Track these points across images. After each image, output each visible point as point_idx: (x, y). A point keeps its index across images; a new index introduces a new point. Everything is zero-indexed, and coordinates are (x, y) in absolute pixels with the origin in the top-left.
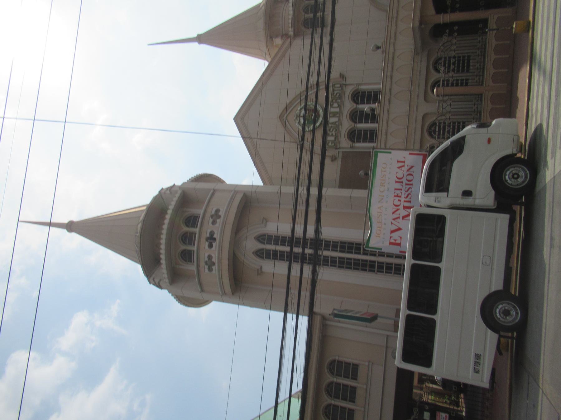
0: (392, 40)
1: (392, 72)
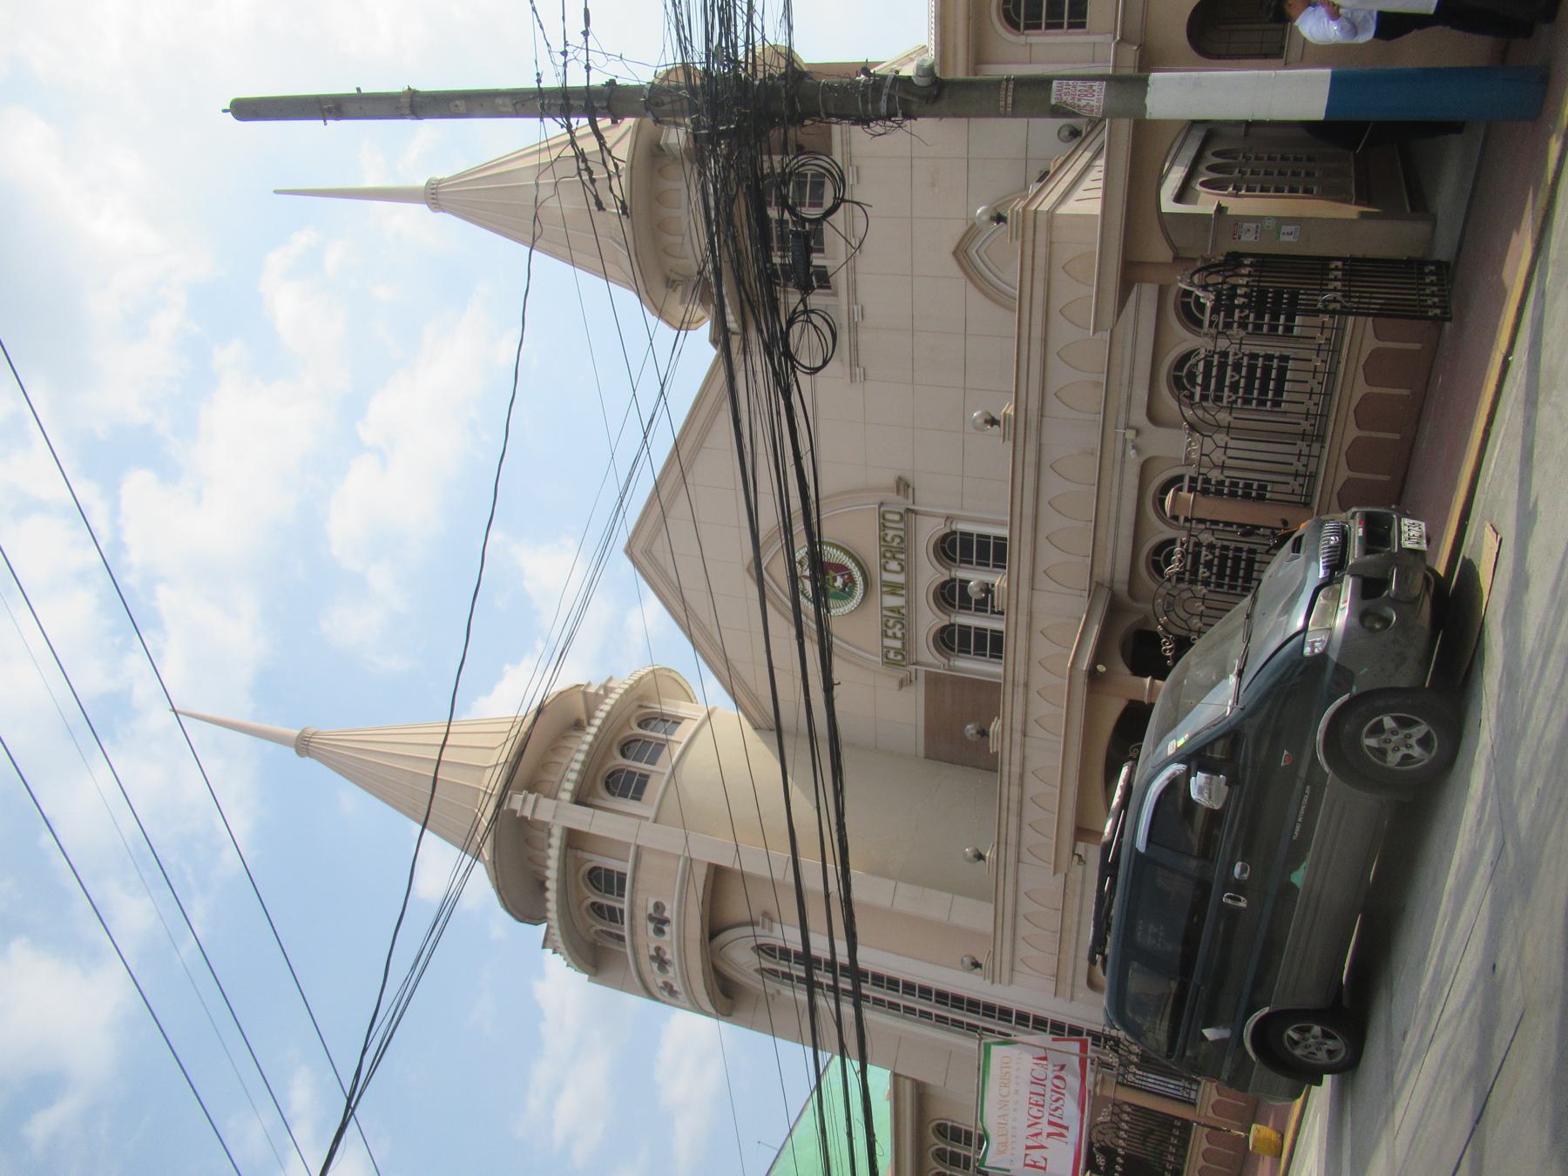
0: (1017, 736)
1: (1021, 802)
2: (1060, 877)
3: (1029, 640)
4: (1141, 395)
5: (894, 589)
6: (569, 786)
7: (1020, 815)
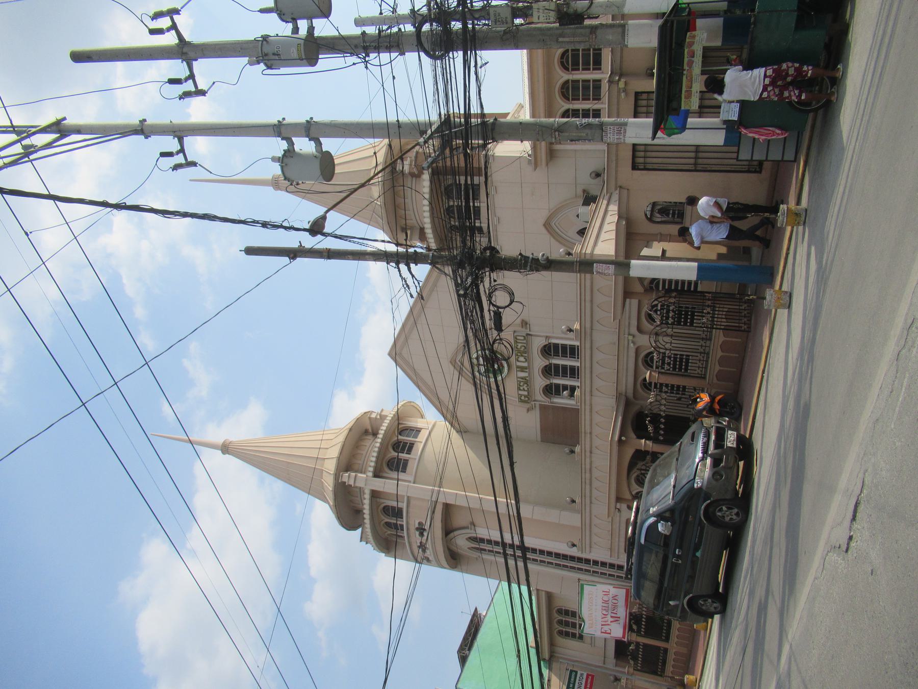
0: (588, 454)
2: (610, 519)
3: (591, 415)
4: (634, 322)
5: (522, 369)
6: (371, 469)
7: (591, 485)
